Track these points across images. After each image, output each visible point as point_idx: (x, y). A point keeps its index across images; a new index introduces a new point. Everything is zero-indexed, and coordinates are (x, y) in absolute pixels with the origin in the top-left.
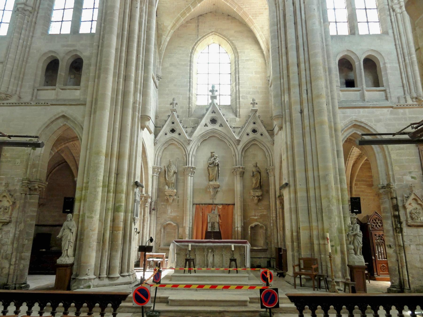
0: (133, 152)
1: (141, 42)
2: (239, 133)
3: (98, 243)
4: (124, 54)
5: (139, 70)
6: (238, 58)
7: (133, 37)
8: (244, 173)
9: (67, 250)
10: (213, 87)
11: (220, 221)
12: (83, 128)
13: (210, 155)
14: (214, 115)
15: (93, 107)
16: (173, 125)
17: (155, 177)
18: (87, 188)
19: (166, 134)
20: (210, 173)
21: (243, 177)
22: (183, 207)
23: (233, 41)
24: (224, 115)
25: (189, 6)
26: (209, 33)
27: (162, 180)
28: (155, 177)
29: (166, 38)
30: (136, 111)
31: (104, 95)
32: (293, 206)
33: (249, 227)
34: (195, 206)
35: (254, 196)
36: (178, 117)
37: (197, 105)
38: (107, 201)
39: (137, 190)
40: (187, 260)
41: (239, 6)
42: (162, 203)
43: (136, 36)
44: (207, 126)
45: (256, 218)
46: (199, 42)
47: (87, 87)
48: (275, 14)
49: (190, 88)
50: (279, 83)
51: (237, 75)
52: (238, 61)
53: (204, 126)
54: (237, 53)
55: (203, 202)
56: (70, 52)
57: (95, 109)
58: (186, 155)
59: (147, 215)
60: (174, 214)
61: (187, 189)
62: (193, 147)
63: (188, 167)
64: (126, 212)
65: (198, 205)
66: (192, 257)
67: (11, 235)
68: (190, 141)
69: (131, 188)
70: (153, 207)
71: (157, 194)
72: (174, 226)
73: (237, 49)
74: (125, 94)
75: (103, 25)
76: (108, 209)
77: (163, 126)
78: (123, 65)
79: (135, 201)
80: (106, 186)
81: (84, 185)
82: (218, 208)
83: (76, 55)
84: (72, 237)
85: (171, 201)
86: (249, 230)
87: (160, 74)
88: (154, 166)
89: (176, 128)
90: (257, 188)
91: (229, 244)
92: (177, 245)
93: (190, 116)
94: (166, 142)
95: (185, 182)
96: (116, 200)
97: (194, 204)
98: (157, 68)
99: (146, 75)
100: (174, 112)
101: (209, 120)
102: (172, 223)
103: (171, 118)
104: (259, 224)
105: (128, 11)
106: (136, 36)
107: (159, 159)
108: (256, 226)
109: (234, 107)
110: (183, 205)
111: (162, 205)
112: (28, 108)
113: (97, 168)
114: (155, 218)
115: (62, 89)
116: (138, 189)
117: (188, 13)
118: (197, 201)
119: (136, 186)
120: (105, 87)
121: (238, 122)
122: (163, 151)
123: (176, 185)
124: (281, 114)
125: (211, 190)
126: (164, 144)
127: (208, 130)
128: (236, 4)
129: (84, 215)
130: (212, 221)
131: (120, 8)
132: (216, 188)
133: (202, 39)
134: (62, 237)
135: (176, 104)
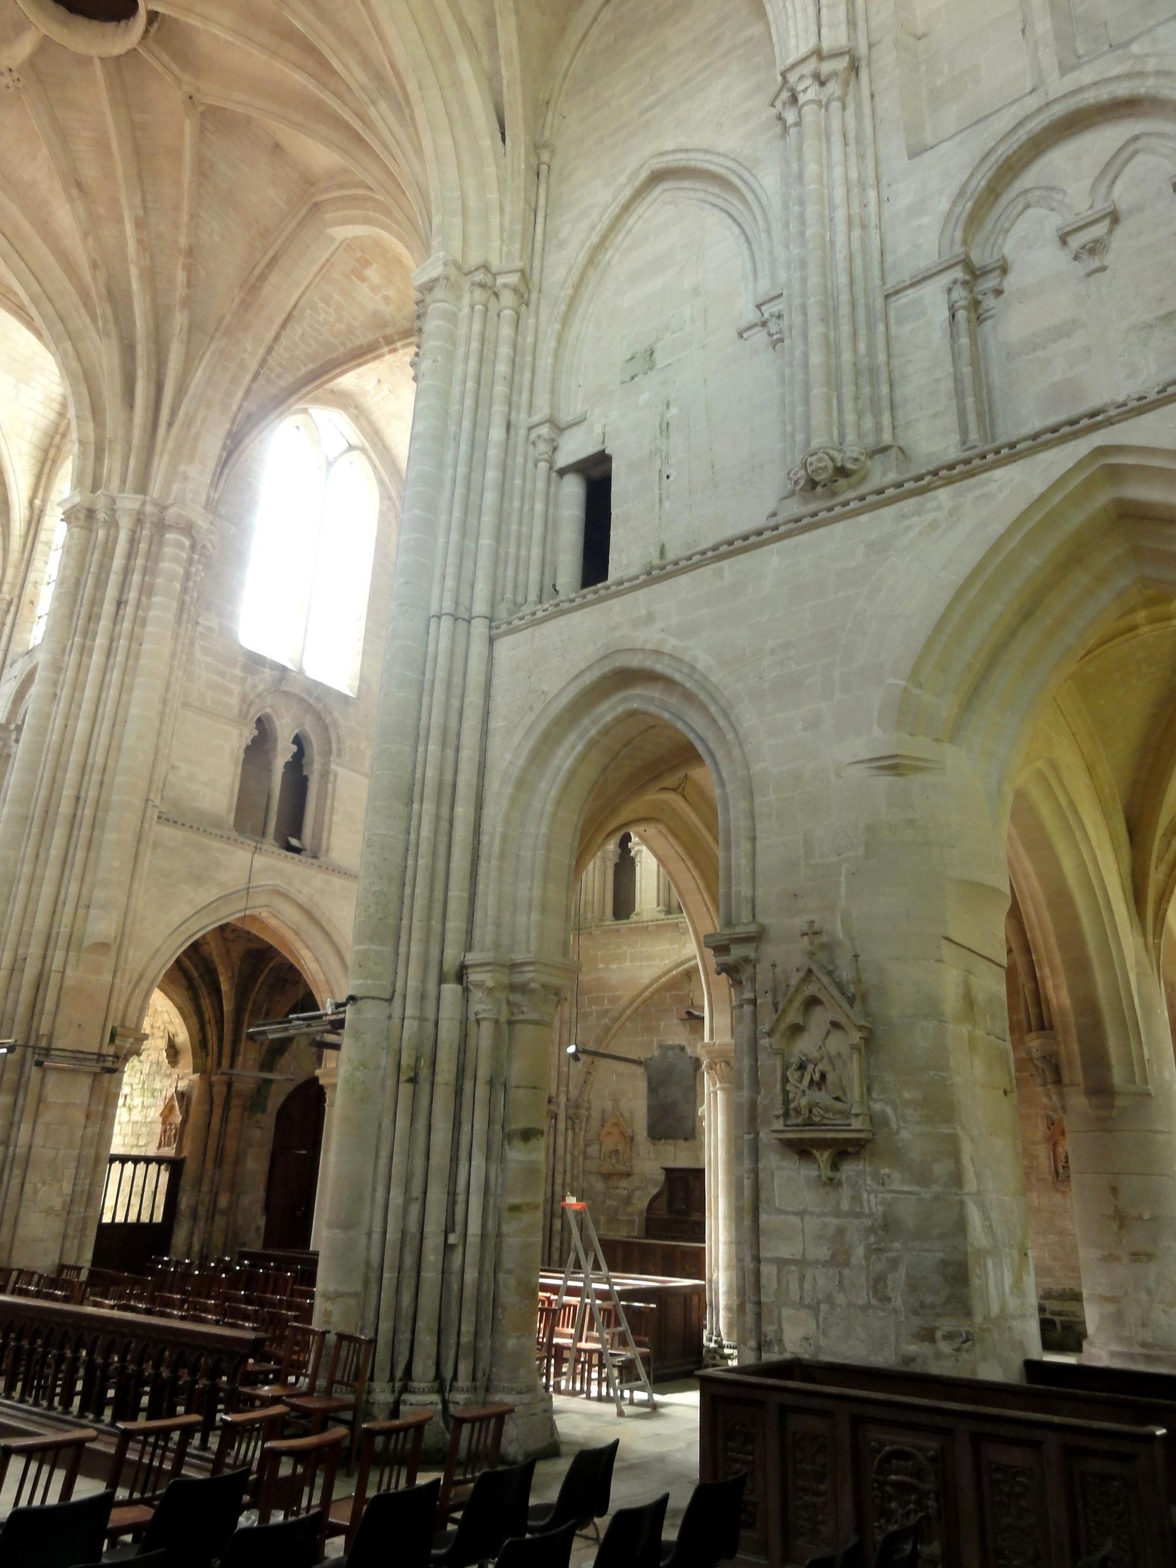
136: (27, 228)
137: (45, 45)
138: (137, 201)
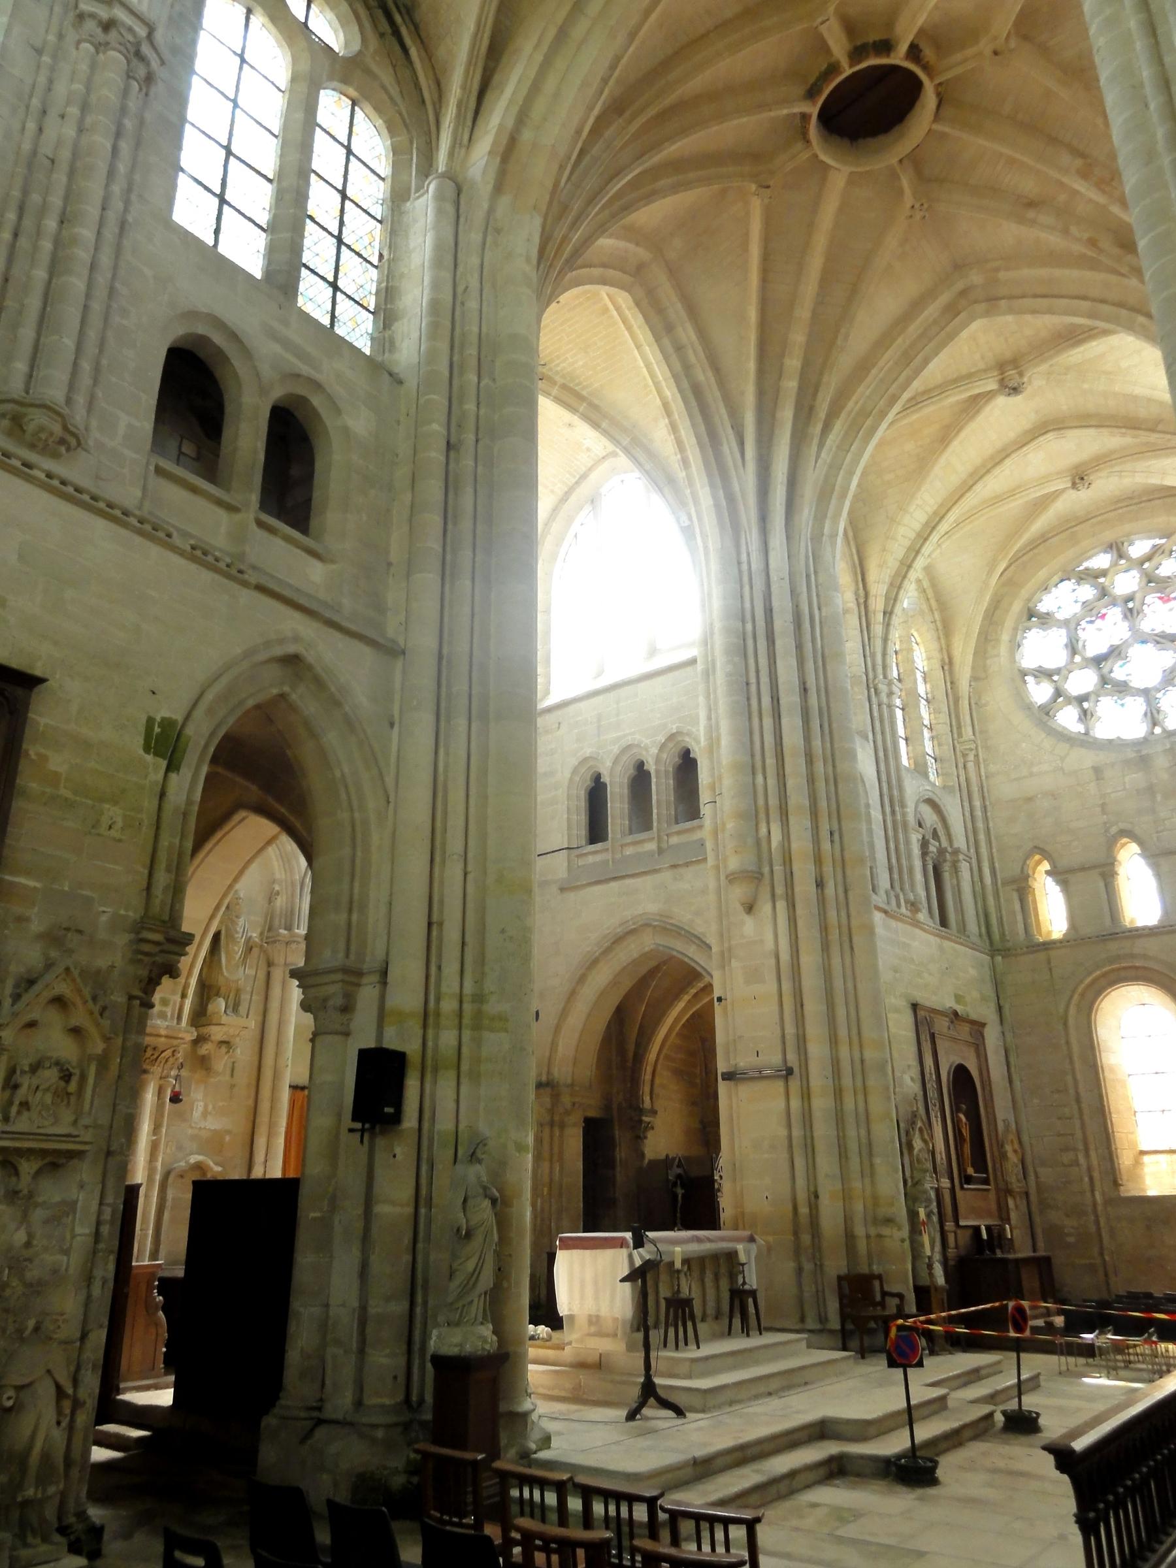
67: (79, 1230)
112: (155, 550)
136: (1043, 272)
137: (915, 160)
138: (1066, 159)
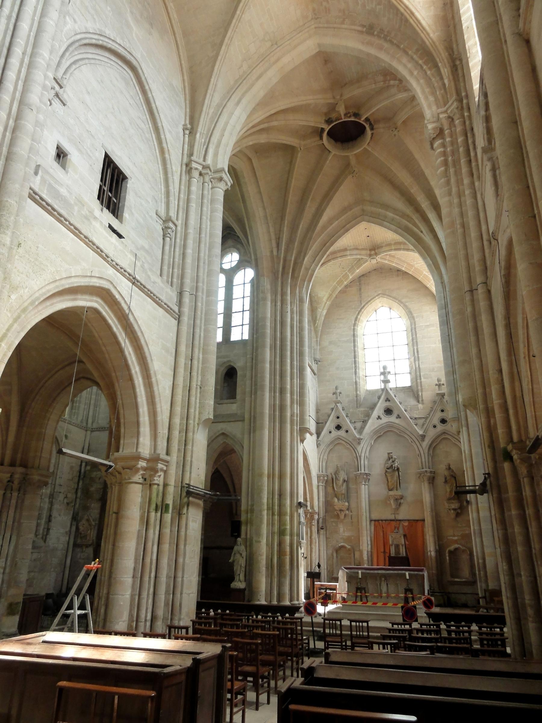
0: (294, 469)
1: (294, 347)
2: (423, 425)
3: (267, 568)
4: (278, 367)
5: (294, 379)
6: (415, 325)
7: (286, 345)
8: (434, 478)
9: (239, 575)
10: (385, 368)
11: (407, 543)
12: (243, 447)
13: (386, 455)
14: (388, 404)
15: (252, 425)
16: (338, 420)
17: (321, 488)
18: (252, 511)
19: (330, 432)
20: (389, 480)
21: (433, 484)
22: (358, 525)
23: (407, 304)
24: (401, 403)
25: (346, 273)
26: (375, 297)
27: (330, 490)
28: (321, 488)
29: (322, 312)
30: (294, 425)
31: (262, 414)
32: (477, 528)
33: (447, 551)
34: (373, 522)
35: (450, 509)
36: (343, 410)
37: (367, 390)
38: (273, 524)
39: (301, 511)
40: (358, 589)
41: (408, 264)
42: (332, 520)
43: (289, 343)
44: (381, 419)
45: (456, 538)
46: (363, 310)
47: (244, 401)
48: (442, 294)
49: (355, 370)
50: (452, 378)
51: (415, 348)
52: (415, 329)
53: (377, 419)
54: (413, 318)
55: (384, 518)
56: (224, 363)
57: (254, 427)
58: (357, 458)
59: (315, 535)
60: (347, 534)
61: (361, 502)
62: (365, 447)
63: (361, 473)
64: (291, 535)
65: (377, 522)
66: (363, 586)
68: (360, 439)
69: (294, 509)
70: (320, 525)
71: (324, 509)
72: (349, 550)
73: (413, 312)
74: (282, 408)
75: (255, 336)
76: (274, 533)
77: (326, 423)
78: (278, 377)
79: (299, 523)
80: (271, 508)
81: (249, 508)
82: (403, 524)
83: (230, 365)
84: (242, 562)
85: (342, 517)
86: (447, 555)
87: (318, 357)
88: (319, 473)
89: (342, 424)
90: (453, 499)
91: (404, 572)
92: (347, 573)
93: (358, 405)
94: (332, 442)
95: (357, 491)
96: (281, 523)
97: (371, 521)
98: (314, 349)
99: (301, 382)
100: (338, 404)
101: (382, 411)
102: (347, 546)
103: (336, 412)
104: (461, 547)
105: (278, 318)
106: (289, 343)
107: (324, 464)
108: (456, 549)
109: (415, 390)
110: (358, 521)
111: (333, 522)
113: (260, 491)
114: (325, 539)
115: (219, 404)
116: (302, 509)
117: (345, 281)
118: (375, 516)
119: (299, 507)
120: (262, 405)
121: (420, 410)
122: (329, 453)
123: (347, 497)
124: (457, 416)
125: (392, 502)
126: (329, 445)
127: (382, 424)
128: (404, 262)
129: (251, 540)
130: (395, 542)
131: (271, 317)
132: (399, 501)
133: (367, 305)
134: (234, 561)
135: (340, 393)
